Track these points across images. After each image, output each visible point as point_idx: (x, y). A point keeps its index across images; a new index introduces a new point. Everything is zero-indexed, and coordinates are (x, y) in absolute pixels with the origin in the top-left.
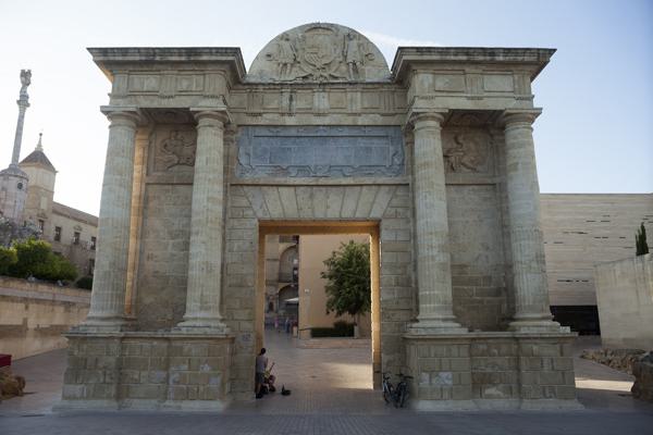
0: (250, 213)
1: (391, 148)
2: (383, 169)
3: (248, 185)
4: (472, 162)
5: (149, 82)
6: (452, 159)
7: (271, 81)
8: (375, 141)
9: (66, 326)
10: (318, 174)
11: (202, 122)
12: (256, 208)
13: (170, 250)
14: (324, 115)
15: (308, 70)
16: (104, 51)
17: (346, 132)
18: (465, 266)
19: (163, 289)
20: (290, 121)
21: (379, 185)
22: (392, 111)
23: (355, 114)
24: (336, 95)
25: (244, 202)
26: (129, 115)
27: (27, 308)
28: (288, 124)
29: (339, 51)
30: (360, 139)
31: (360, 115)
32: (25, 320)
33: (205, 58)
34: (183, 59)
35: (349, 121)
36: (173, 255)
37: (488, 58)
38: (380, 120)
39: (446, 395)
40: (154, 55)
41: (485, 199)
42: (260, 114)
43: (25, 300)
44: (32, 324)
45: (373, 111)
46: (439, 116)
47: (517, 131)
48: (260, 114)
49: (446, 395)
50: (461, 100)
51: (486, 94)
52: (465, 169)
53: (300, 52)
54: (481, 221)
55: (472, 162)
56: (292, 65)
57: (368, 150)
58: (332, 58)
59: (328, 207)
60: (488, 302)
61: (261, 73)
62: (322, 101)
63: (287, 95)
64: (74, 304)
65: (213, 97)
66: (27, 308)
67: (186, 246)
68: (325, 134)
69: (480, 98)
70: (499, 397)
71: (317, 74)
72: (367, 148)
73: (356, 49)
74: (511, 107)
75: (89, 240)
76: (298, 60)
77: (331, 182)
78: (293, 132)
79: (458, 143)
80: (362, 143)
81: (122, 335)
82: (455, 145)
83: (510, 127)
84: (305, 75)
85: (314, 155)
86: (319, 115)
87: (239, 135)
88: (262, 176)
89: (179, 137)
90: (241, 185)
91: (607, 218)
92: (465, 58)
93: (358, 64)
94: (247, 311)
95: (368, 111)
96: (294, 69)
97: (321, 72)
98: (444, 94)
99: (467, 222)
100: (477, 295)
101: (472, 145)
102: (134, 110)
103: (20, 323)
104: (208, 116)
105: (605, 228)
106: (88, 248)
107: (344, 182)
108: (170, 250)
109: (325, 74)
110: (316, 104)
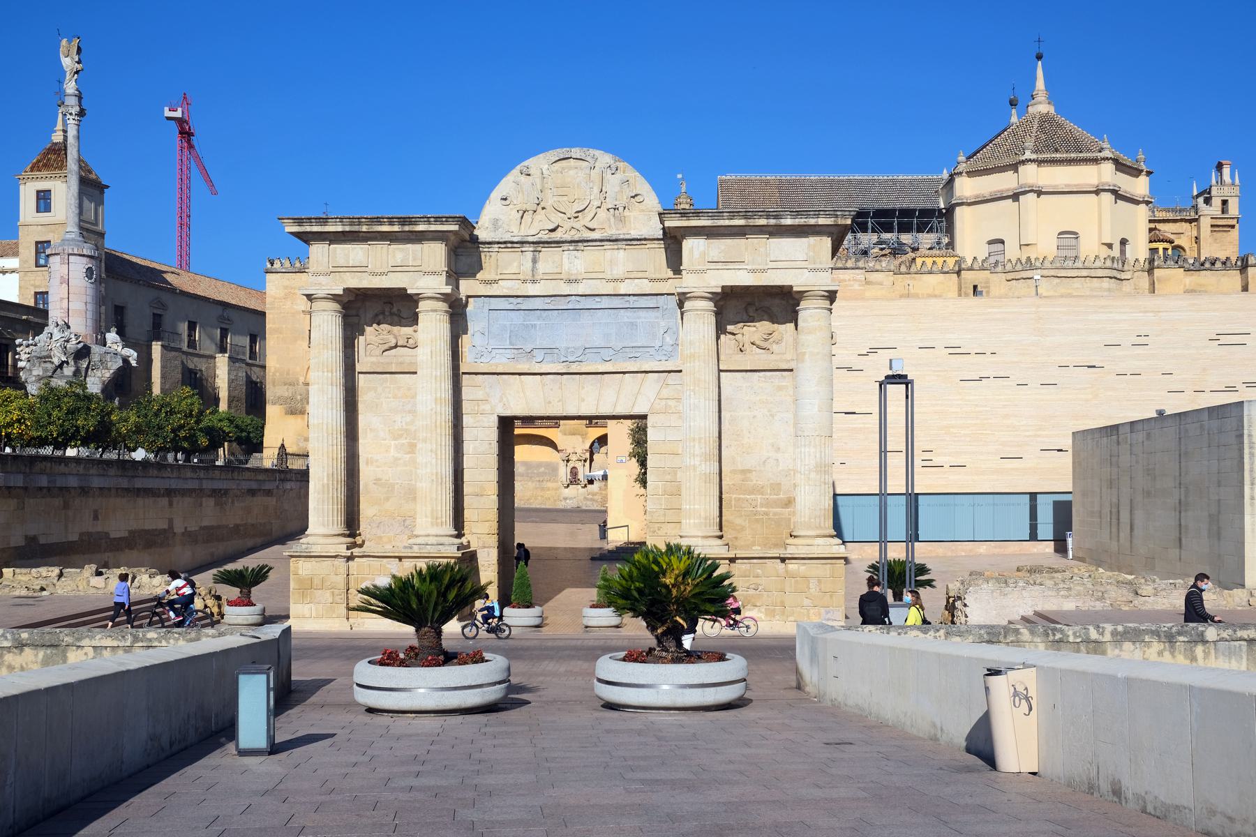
0: (487, 407)
1: (663, 324)
2: (652, 351)
7: (507, 237)
8: (642, 313)
9: (219, 527)
11: (422, 305)
13: (393, 452)
15: (557, 219)
17: (606, 303)
18: (750, 471)
19: (387, 499)
20: (531, 289)
23: (616, 280)
25: (480, 394)
26: (335, 298)
27: (171, 504)
29: (596, 190)
31: (622, 281)
33: (421, 227)
34: (396, 228)
36: (397, 459)
37: (772, 222)
38: (647, 287)
40: (360, 224)
41: (780, 388)
42: (496, 282)
43: (169, 493)
45: (640, 275)
47: (808, 312)
48: (496, 282)
53: (549, 193)
54: (772, 416)
57: (633, 325)
59: (583, 400)
60: (775, 514)
62: (574, 262)
63: (529, 255)
64: (226, 492)
65: (434, 273)
66: (171, 504)
67: (412, 448)
69: (764, 271)
72: (632, 323)
73: (617, 189)
76: (542, 204)
78: (537, 304)
79: (746, 309)
81: (348, 553)
82: (745, 317)
83: (803, 304)
85: (569, 334)
86: (570, 281)
88: (501, 362)
89: (395, 310)
91: (1142, 340)
92: (741, 222)
93: (621, 209)
97: (573, 223)
98: (719, 266)
103: (166, 527)
108: (393, 452)
109: (577, 225)
110: (566, 266)
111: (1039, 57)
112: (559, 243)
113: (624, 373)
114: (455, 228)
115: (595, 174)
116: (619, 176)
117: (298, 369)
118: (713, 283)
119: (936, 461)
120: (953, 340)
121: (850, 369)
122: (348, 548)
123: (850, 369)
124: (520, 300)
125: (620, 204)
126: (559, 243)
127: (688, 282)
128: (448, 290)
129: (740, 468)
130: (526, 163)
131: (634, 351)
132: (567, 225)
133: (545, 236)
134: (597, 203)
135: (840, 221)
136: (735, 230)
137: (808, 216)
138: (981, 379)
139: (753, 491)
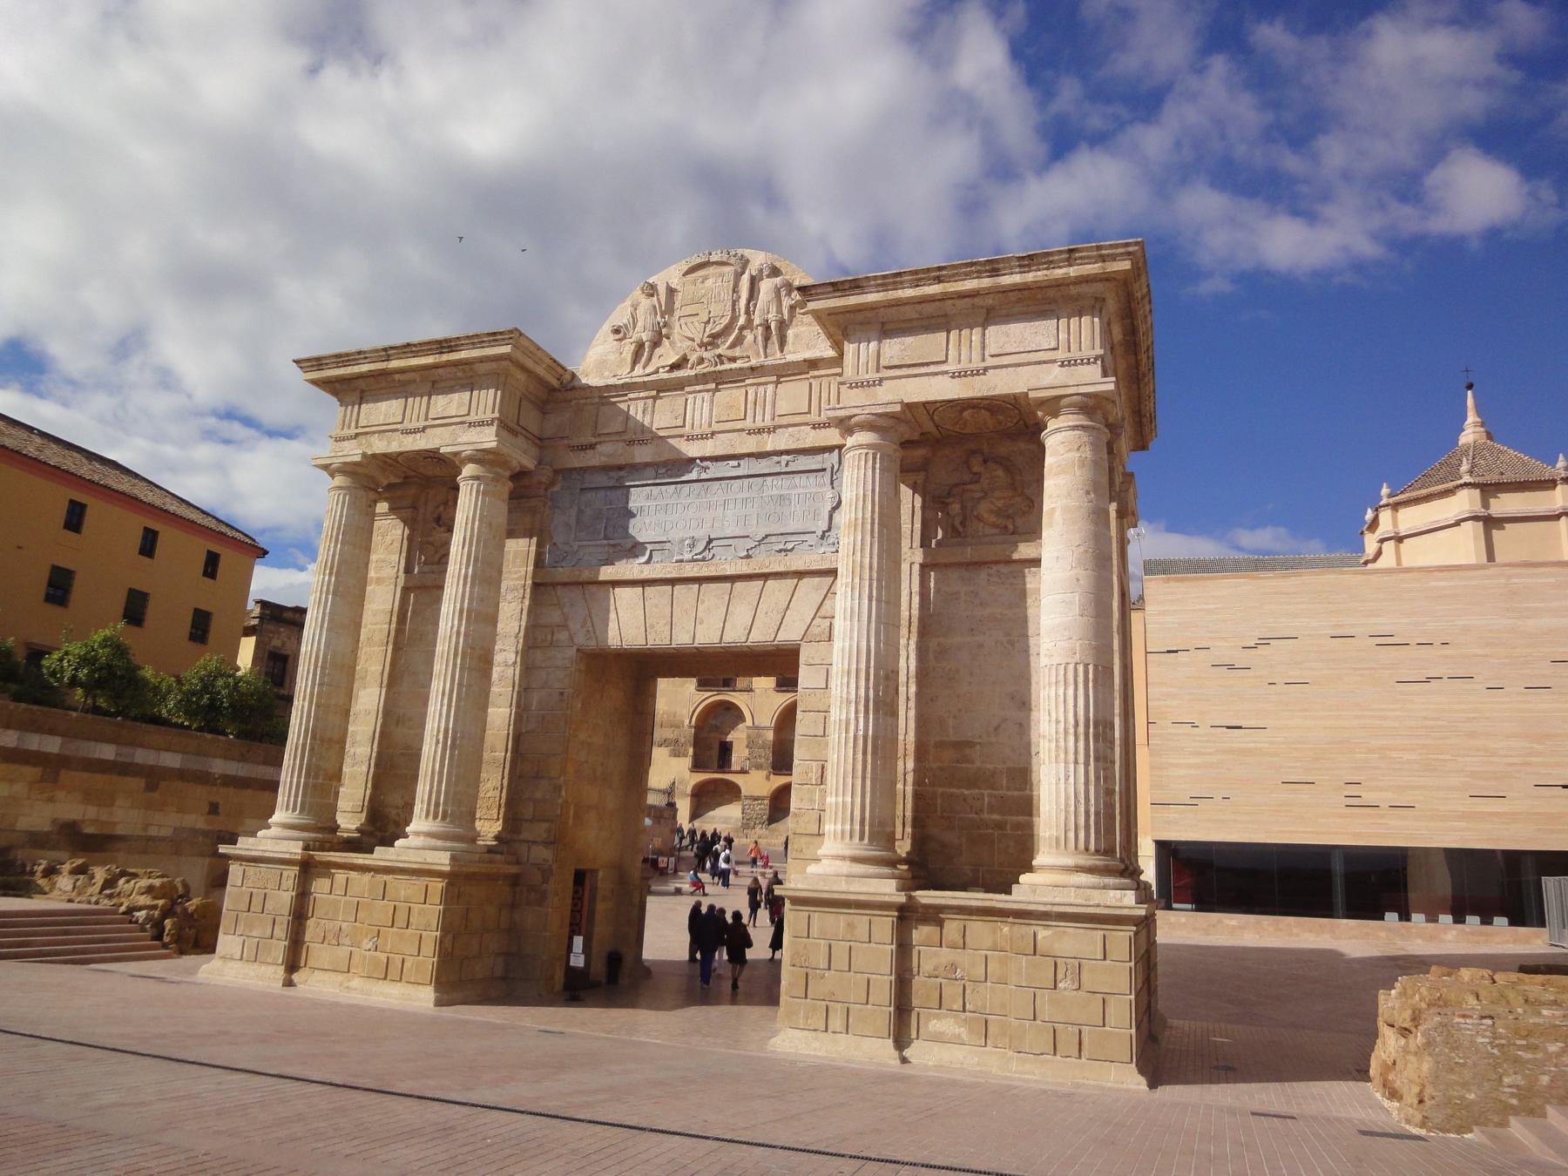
0: (562, 636)
1: (829, 494)
3: (565, 584)
4: (998, 513)
6: (956, 508)
10: (687, 556)
12: (574, 626)
14: (703, 437)
16: (317, 363)
17: (746, 467)
18: (970, 744)
21: (800, 574)
23: (760, 431)
24: (731, 396)
25: (555, 617)
28: (638, 460)
30: (769, 479)
31: (771, 430)
34: (430, 360)
35: (750, 444)
37: (986, 282)
39: (837, 1022)
42: (592, 446)
45: (798, 419)
46: (891, 422)
49: (837, 1022)
50: (933, 380)
51: (990, 362)
52: (989, 531)
55: (998, 513)
56: (656, 344)
58: (726, 321)
65: (481, 424)
68: (704, 476)
69: (976, 373)
70: (957, 1041)
71: (693, 358)
74: (1046, 382)
76: (664, 331)
77: (705, 572)
80: (773, 486)
84: (673, 359)
86: (690, 438)
87: (556, 488)
90: (554, 585)
94: (545, 825)
95: (785, 421)
96: (658, 351)
99: (981, 646)
100: (991, 810)
101: (1000, 473)
102: (358, 459)
104: (471, 459)
107: (730, 570)
111: (1470, 387)
113: (765, 577)
115: (745, 278)
116: (778, 280)
117: (685, 711)
119: (1369, 797)
120: (1382, 624)
121: (1231, 667)
122: (306, 848)
123: (1231, 667)
124: (622, 473)
125: (772, 317)
126: (679, 385)
129: (953, 738)
131: (787, 541)
132: (693, 358)
133: (663, 375)
134: (742, 320)
136: (929, 309)
137: (1051, 265)
138: (1428, 680)
139: (974, 781)
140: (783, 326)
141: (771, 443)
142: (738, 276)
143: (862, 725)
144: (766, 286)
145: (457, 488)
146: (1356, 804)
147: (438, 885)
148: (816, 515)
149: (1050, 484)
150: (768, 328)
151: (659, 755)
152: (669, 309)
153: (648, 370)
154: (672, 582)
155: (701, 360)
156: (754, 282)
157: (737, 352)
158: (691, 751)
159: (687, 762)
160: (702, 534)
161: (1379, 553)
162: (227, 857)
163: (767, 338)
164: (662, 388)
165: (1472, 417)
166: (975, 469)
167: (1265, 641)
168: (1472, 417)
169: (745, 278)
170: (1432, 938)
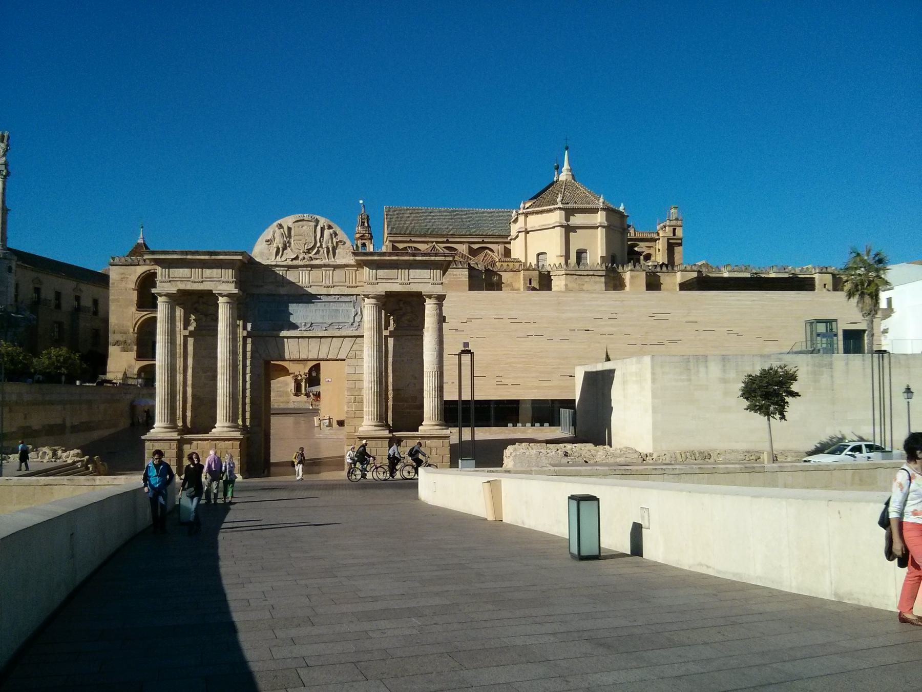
5: (183, 272)
21: (345, 337)
22: (354, 284)
24: (316, 273)
32: (64, 420)
37: (411, 258)
42: (262, 286)
44: (68, 424)
56: (285, 248)
61: (262, 254)
65: (228, 282)
75: (51, 296)
80: (333, 306)
81: (179, 437)
105: (612, 325)
106: (53, 307)
111: (567, 148)
112: (296, 267)
113: (332, 337)
114: (240, 258)
118: (380, 290)
119: (505, 381)
120: (513, 314)
121: (457, 330)
123: (457, 330)
126: (296, 267)
127: (369, 290)
128: (236, 291)
130: (279, 222)
132: (301, 257)
133: (290, 263)
135: (448, 259)
140: (334, 249)
141: (332, 291)
142: (316, 226)
143: (375, 388)
144: (327, 232)
145: (217, 305)
146: (500, 384)
147: (238, 443)
148: (349, 317)
149: (427, 319)
150: (328, 248)
151: (113, 350)
152: (290, 236)
153: (283, 259)
154: (298, 338)
155: (304, 258)
156: (322, 229)
157: (317, 256)
158: (135, 348)
159: (133, 354)
160: (309, 321)
161: (517, 236)
162: (144, 440)
163: (328, 252)
164: (290, 267)
165: (566, 165)
166: (401, 305)
167: (470, 320)
168: (566, 165)
169: (319, 228)
170: (523, 432)
